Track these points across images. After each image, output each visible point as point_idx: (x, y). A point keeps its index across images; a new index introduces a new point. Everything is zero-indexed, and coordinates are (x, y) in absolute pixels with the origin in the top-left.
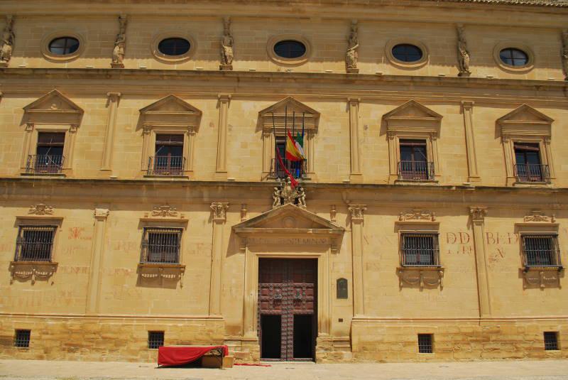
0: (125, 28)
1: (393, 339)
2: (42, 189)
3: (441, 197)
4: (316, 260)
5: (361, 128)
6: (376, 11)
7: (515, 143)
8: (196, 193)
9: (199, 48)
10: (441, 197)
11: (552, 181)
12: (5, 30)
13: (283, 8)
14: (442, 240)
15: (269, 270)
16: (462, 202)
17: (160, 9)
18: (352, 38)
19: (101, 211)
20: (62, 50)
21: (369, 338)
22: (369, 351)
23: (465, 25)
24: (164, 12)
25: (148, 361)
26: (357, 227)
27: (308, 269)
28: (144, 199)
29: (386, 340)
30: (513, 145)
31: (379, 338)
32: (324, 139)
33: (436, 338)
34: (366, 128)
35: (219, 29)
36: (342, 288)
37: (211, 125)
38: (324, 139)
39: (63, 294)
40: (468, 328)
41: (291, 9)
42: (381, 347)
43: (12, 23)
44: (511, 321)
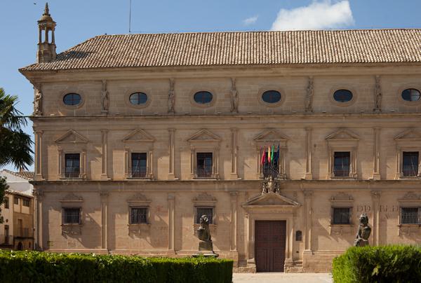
0: (173, 86)
2: (138, 186)
3: (356, 186)
4: (285, 221)
5: (313, 147)
6: (324, 70)
8: (221, 186)
9: (218, 98)
10: (356, 186)
12: (103, 89)
14: (355, 209)
15: (259, 225)
16: (367, 188)
17: (194, 74)
18: (309, 88)
20: (137, 101)
21: (311, 261)
22: (310, 268)
23: (381, 75)
24: (196, 76)
26: (308, 201)
28: (193, 190)
32: (291, 153)
34: (315, 146)
35: (229, 84)
36: (298, 236)
37: (227, 146)
38: (291, 153)
39: (155, 241)
41: (272, 72)
43: (106, 85)
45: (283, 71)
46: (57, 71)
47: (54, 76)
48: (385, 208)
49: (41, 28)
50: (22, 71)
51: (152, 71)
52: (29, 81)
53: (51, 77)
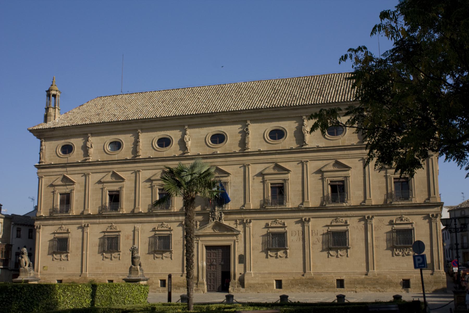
1: (263, 282)
6: (258, 115)
7: (331, 181)
11: (348, 201)
13: (212, 118)
19: (138, 226)
21: (252, 282)
25: (160, 292)
27: (226, 250)
29: (260, 282)
30: (329, 182)
31: (257, 282)
32: (234, 186)
33: (283, 282)
38: (234, 186)
39: (125, 264)
40: (299, 277)
42: (258, 286)
44: (320, 274)
45: (224, 117)
46: (54, 128)
47: (53, 133)
48: (316, 232)
49: (49, 95)
50: (31, 131)
51: (123, 124)
52: (36, 137)
53: (51, 133)
